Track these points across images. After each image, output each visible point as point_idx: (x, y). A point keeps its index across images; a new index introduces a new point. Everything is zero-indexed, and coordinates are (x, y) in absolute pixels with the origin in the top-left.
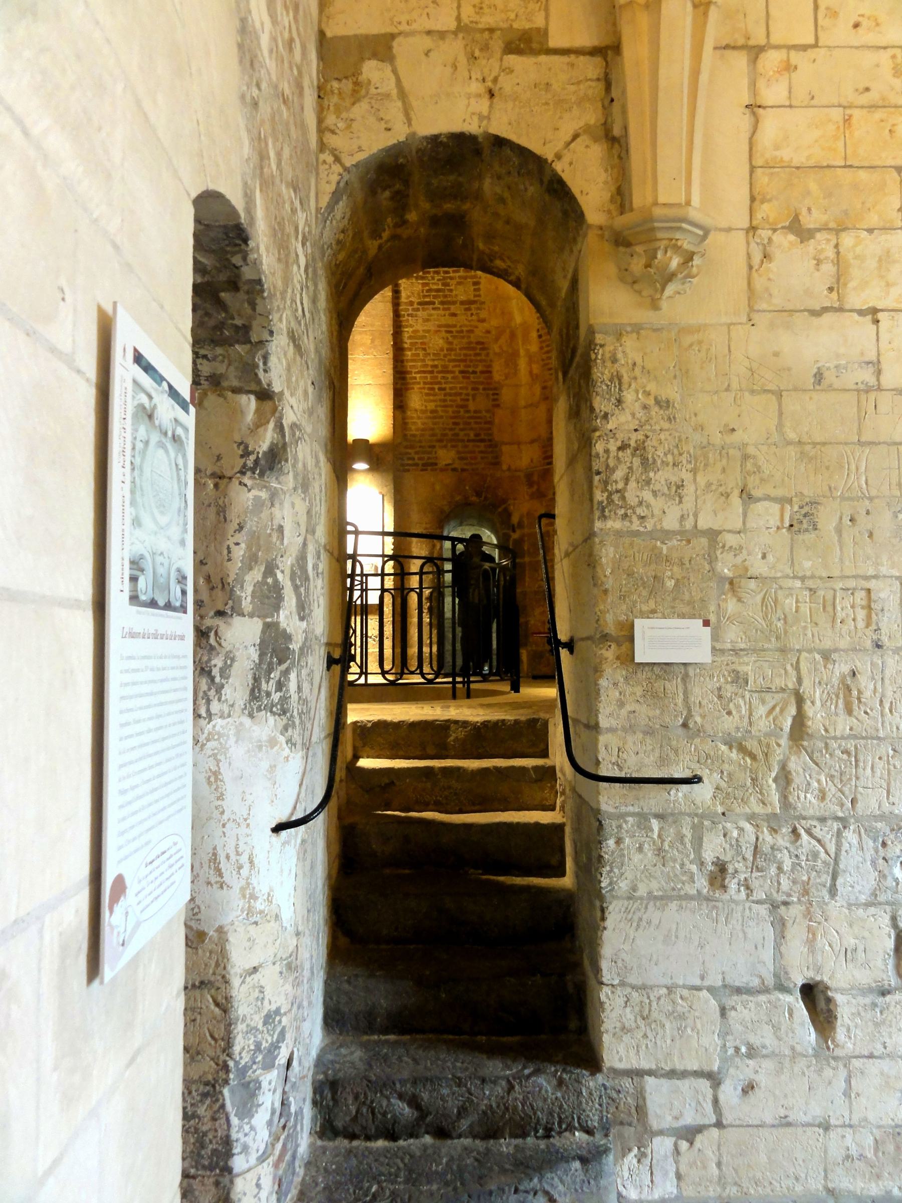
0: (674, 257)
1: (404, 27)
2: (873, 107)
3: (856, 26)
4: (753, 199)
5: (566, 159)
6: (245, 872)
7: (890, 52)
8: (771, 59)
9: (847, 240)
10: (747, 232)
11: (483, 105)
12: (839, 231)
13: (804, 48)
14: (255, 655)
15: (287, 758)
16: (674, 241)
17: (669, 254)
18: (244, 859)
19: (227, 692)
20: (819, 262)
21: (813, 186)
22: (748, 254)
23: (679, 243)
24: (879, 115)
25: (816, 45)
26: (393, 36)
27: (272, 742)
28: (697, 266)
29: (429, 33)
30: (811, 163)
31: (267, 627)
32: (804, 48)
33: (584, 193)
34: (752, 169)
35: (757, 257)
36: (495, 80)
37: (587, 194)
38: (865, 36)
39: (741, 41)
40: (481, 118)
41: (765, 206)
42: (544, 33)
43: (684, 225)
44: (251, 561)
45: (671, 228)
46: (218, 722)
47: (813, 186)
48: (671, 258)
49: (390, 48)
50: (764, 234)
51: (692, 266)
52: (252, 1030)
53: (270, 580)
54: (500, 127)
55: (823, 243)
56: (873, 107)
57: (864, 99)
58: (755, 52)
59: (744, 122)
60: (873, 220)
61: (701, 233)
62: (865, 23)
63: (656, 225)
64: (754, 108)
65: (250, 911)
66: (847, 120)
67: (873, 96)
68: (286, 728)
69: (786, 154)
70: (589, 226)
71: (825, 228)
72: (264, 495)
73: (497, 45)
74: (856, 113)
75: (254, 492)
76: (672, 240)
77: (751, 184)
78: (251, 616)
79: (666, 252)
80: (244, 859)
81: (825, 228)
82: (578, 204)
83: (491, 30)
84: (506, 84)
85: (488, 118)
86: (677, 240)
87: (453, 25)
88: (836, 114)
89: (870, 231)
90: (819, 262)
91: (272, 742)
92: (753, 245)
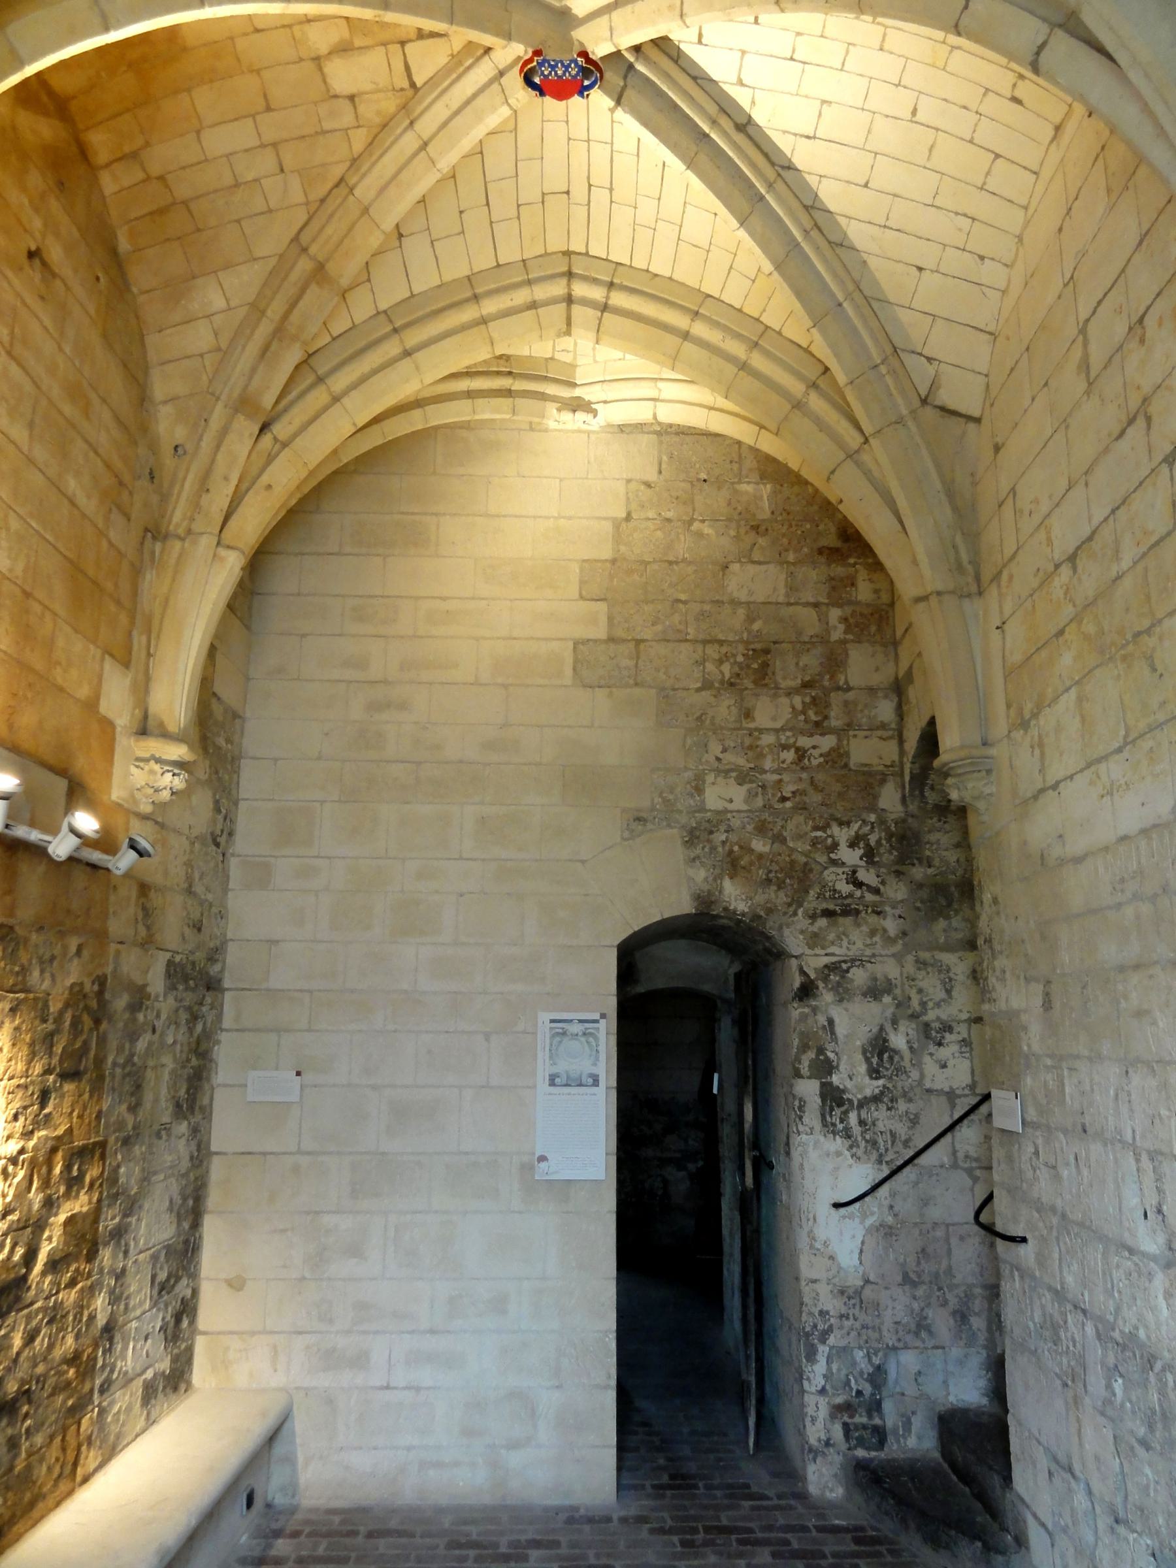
6: (811, 1223)
14: (819, 1101)
15: (850, 1166)
18: (811, 1216)
19: (806, 1120)
27: (838, 1154)
31: (823, 1085)
44: (804, 1048)
46: (804, 1137)
52: (811, 1314)
53: (822, 1057)
65: (812, 1247)
68: (851, 1147)
72: (806, 1010)
75: (800, 1010)
78: (809, 1078)
80: (811, 1216)
91: (838, 1154)
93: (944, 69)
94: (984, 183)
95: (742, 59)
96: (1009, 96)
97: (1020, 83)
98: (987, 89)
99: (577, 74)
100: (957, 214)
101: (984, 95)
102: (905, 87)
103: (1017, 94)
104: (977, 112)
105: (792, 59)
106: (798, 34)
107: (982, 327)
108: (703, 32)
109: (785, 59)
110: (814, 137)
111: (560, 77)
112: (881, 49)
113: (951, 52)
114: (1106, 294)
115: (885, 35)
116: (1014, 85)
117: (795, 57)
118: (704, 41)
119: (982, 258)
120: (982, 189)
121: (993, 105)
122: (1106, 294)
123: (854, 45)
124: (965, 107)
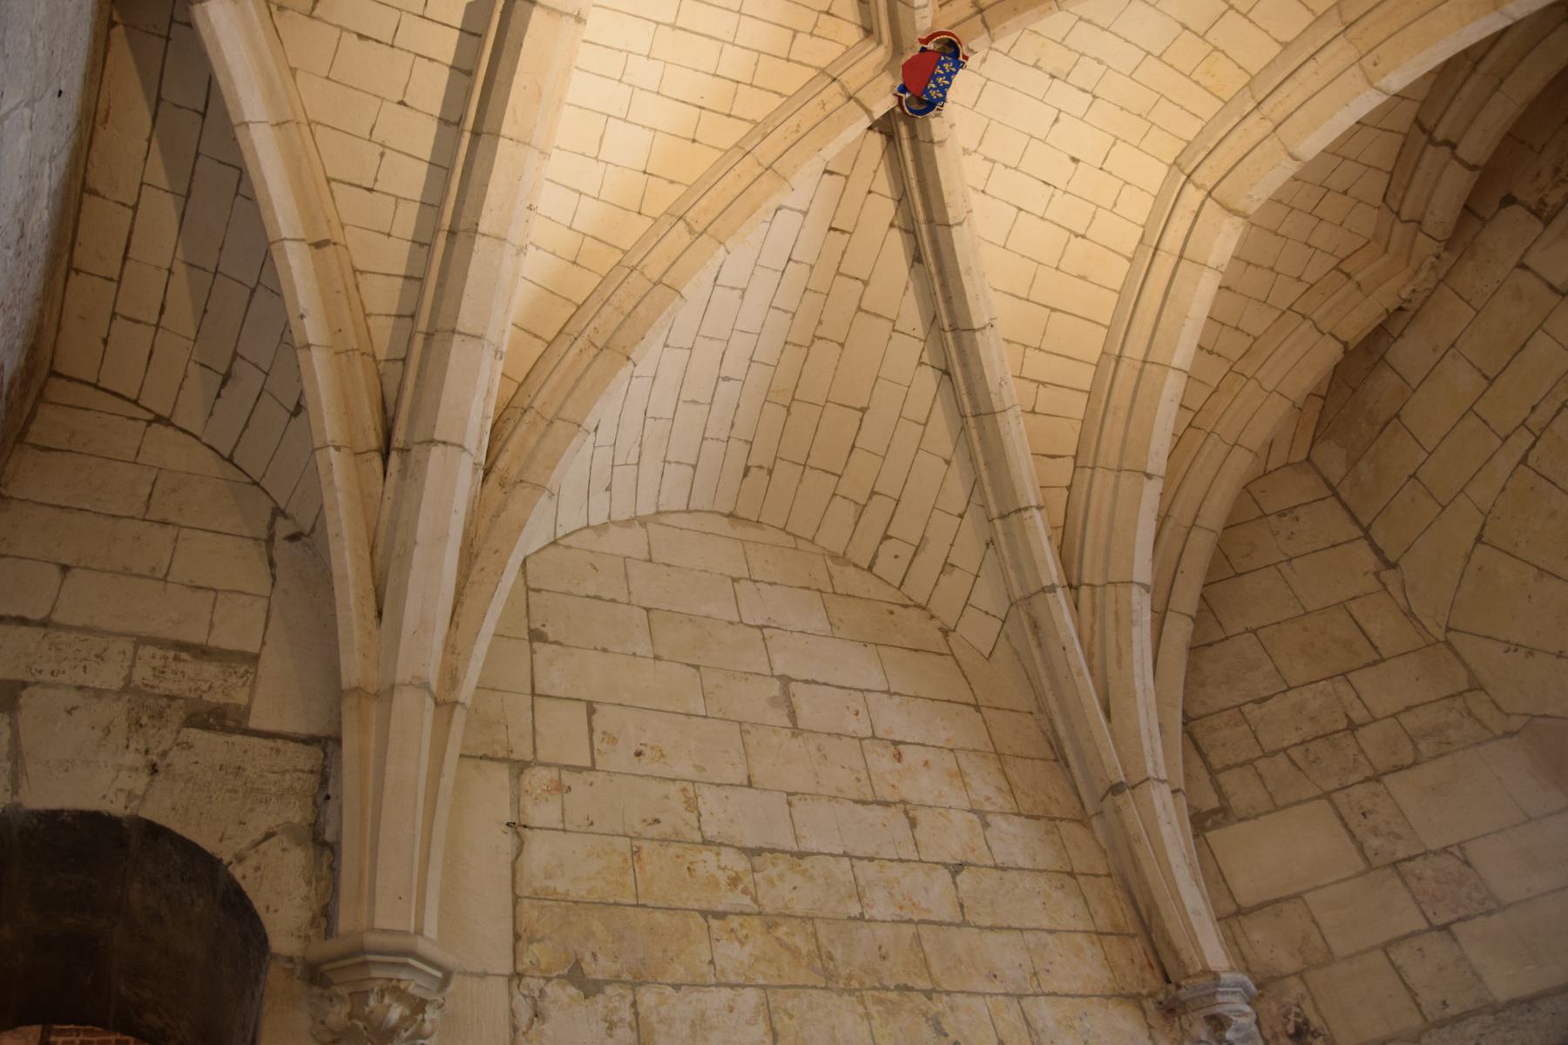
0: (395, 1005)
1: (46, 677)
2: (665, 841)
3: (639, 754)
4: (517, 937)
5: (251, 862)
7: (679, 785)
8: (538, 778)
9: (648, 998)
10: (510, 981)
11: (140, 782)
12: (637, 983)
13: (579, 769)
16: (394, 983)
17: (387, 1000)
20: (611, 1026)
21: (597, 927)
22: (512, 1010)
23: (402, 985)
24: (673, 850)
25: (593, 768)
26: (24, 685)
28: (432, 1021)
29: (80, 688)
30: (594, 897)
32: (579, 769)
33: (272, 909)
34: (516, 900)
35: (524, 1016)
36: (164, 754)
37: (276, 911)
38: (647, 765)
39: (502, 754)
40: (130, 795)
41: (535, 947)
42: (246, 711)
43: (411, 961)
45: (393, 964)
47: (597, 927)
48: (389, 1006)
49: (16, 697)
50: (534, 983)
51: (423, 1020)
54: (157, 811)
55: (616, 1000)
56: (665, 841)
57: (654, 831)
58: (519, 767)
59: (507, 842)
60: (679, 972)
61: (439, 974)
62: (647, 751)
63: (370, 958)
64: (517, 827)
66: (636, 853)
67: (664, 828)
69: (560, 885)
70: (275, 956)
71: (616, 980)
73: (176, 715)
74: (646, 845)
76: (391, 980)
77: (515, 918)
79: (383, 997)
81: (616, 980)
82: (261, 926)
83: (171, 698)
84: (179, 760)
85: (143, 798)
86: (399, 980)
87: (117, 684)
88: (622, 844)
89: (677, 987)
90: (611, 1026)
92: (518, 998)
93: (766, 400)
94: (669, 462)
95: (800, 211)
96: (749, 464)
97: (765, 472)
98: (751, 443)
99: (929, 95)
100: (640, 446)
101: (746, 441)
102: (749, 366)
103: (753, 471)
104: (729, 438)
105: (789, 259)
106: (812, 267)
107: (559, 523)
108: (834, 177)
109: (791, 254)
110: (715, 285)
111: (934, 77)
112: (786, 343)
113: (784, 406)
114: (825, 684)
115: (801, 346)
116: (761, 467)
117: (791, 262)
118: (826, 175)
119: (609, 489)
120: (665, 461)
121: (738, 452)
122: (825, 684)
123: (793, 318)
124: (733, 425)
